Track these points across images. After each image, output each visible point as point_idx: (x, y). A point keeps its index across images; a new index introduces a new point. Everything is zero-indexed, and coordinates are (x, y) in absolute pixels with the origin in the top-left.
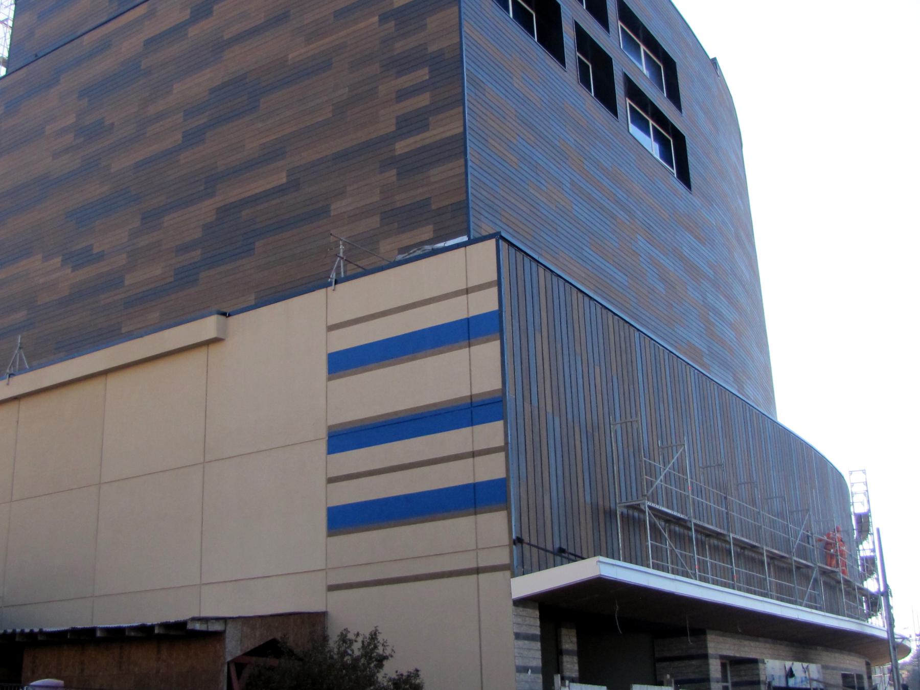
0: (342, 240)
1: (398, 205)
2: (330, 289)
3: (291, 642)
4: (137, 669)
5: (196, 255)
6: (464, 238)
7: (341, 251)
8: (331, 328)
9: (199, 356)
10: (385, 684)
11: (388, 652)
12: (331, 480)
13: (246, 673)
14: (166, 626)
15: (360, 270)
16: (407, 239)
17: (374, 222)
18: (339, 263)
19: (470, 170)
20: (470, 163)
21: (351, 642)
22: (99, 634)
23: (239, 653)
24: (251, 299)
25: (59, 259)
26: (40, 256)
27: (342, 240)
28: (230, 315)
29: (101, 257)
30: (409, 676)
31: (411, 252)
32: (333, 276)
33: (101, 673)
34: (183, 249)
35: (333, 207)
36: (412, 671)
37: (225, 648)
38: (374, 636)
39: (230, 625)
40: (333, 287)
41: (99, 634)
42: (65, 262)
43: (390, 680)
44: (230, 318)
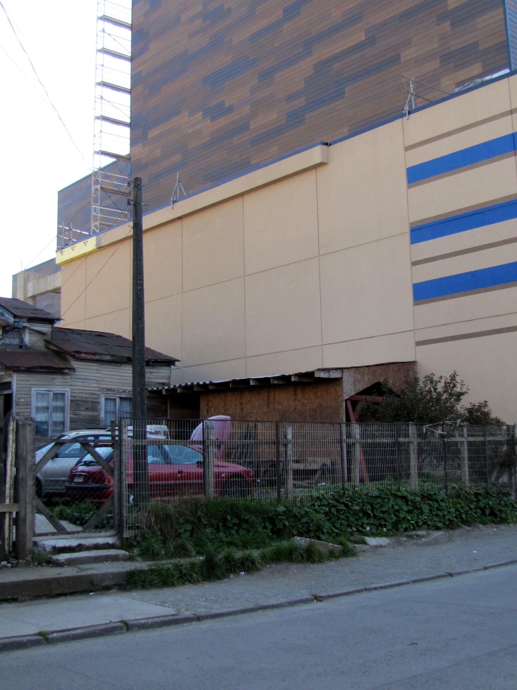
0: (411, 80)
1: (453, 49)
2: (405, 118)
3: (390, 383)
4: (280, 407)
5: (301, 101)
6: (507, 71)
7: (412, 89)
8: (408, 148)
9: (311, 176)
10: (462, 412)
11: (464, 390)
12: (415, 263)
13: (359, 407)
14: (300, 375)
15: (427, 102)
16: (462, 75)
17: (434, 65)
18: (411, 96)
19: (508, 16)
20: (508, 11)
21: (437, 382)
22: (252, 383)
23: (353, 393)
24: (345, 131)
25: (200, 114)
26: (187, 113)
27: (411, 80)
28: (330, 145)
29: (230, 109)
30: (480, 406)
31: (465, 85)
32: (407, 108)
33: (255, 411)
34: (290, 98)
35: (402, 55)
36: (477, 404)
37: (343, 390)
38: (453, 377)
39: (346, 372)
40: (407, 117)
41: (252, 383)
42: (205, 115)
43: (467, 409)
44: (331, 147)
